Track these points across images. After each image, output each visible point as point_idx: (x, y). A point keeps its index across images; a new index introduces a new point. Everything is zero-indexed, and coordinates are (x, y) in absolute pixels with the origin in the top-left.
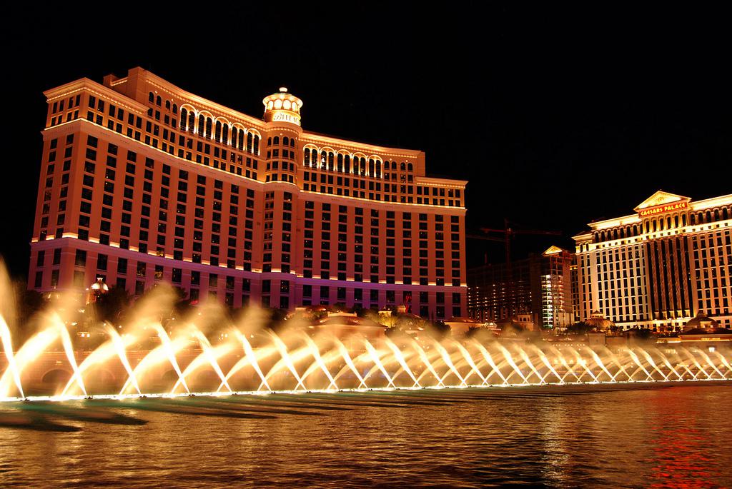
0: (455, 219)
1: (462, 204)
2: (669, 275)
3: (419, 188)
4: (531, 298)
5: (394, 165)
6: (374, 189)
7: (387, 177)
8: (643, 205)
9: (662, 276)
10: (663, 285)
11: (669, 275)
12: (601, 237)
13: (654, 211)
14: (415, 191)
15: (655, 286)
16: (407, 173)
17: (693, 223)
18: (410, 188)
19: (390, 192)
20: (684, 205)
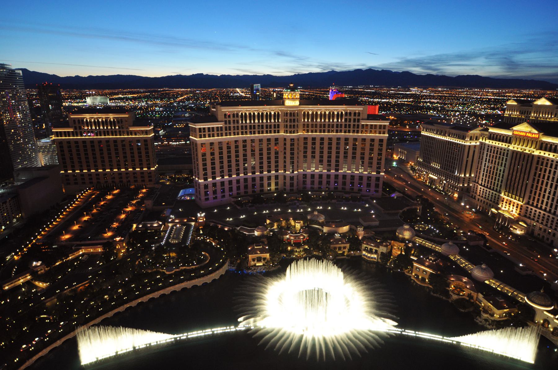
0: (381, 140)
1: (386, 132)
2: (518, 175)
3: (363, 125)
4: (373, 214)
5: (350, 113)
6: (338, 128)
7: (346, 120)
8: (515, 128)
9: (514, 173)
10: (513, 179)
11: (518, 175)
12: (493, 137)
13: (521, 134)
14: (360, 127)
15: (510, 177)
16: (357, 118)
17: (541, 149)
18: (358, 126)
19: (347, 128)
20: (537, 136)
